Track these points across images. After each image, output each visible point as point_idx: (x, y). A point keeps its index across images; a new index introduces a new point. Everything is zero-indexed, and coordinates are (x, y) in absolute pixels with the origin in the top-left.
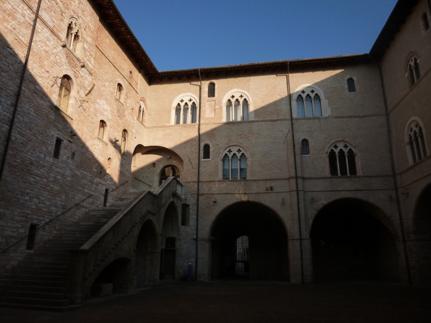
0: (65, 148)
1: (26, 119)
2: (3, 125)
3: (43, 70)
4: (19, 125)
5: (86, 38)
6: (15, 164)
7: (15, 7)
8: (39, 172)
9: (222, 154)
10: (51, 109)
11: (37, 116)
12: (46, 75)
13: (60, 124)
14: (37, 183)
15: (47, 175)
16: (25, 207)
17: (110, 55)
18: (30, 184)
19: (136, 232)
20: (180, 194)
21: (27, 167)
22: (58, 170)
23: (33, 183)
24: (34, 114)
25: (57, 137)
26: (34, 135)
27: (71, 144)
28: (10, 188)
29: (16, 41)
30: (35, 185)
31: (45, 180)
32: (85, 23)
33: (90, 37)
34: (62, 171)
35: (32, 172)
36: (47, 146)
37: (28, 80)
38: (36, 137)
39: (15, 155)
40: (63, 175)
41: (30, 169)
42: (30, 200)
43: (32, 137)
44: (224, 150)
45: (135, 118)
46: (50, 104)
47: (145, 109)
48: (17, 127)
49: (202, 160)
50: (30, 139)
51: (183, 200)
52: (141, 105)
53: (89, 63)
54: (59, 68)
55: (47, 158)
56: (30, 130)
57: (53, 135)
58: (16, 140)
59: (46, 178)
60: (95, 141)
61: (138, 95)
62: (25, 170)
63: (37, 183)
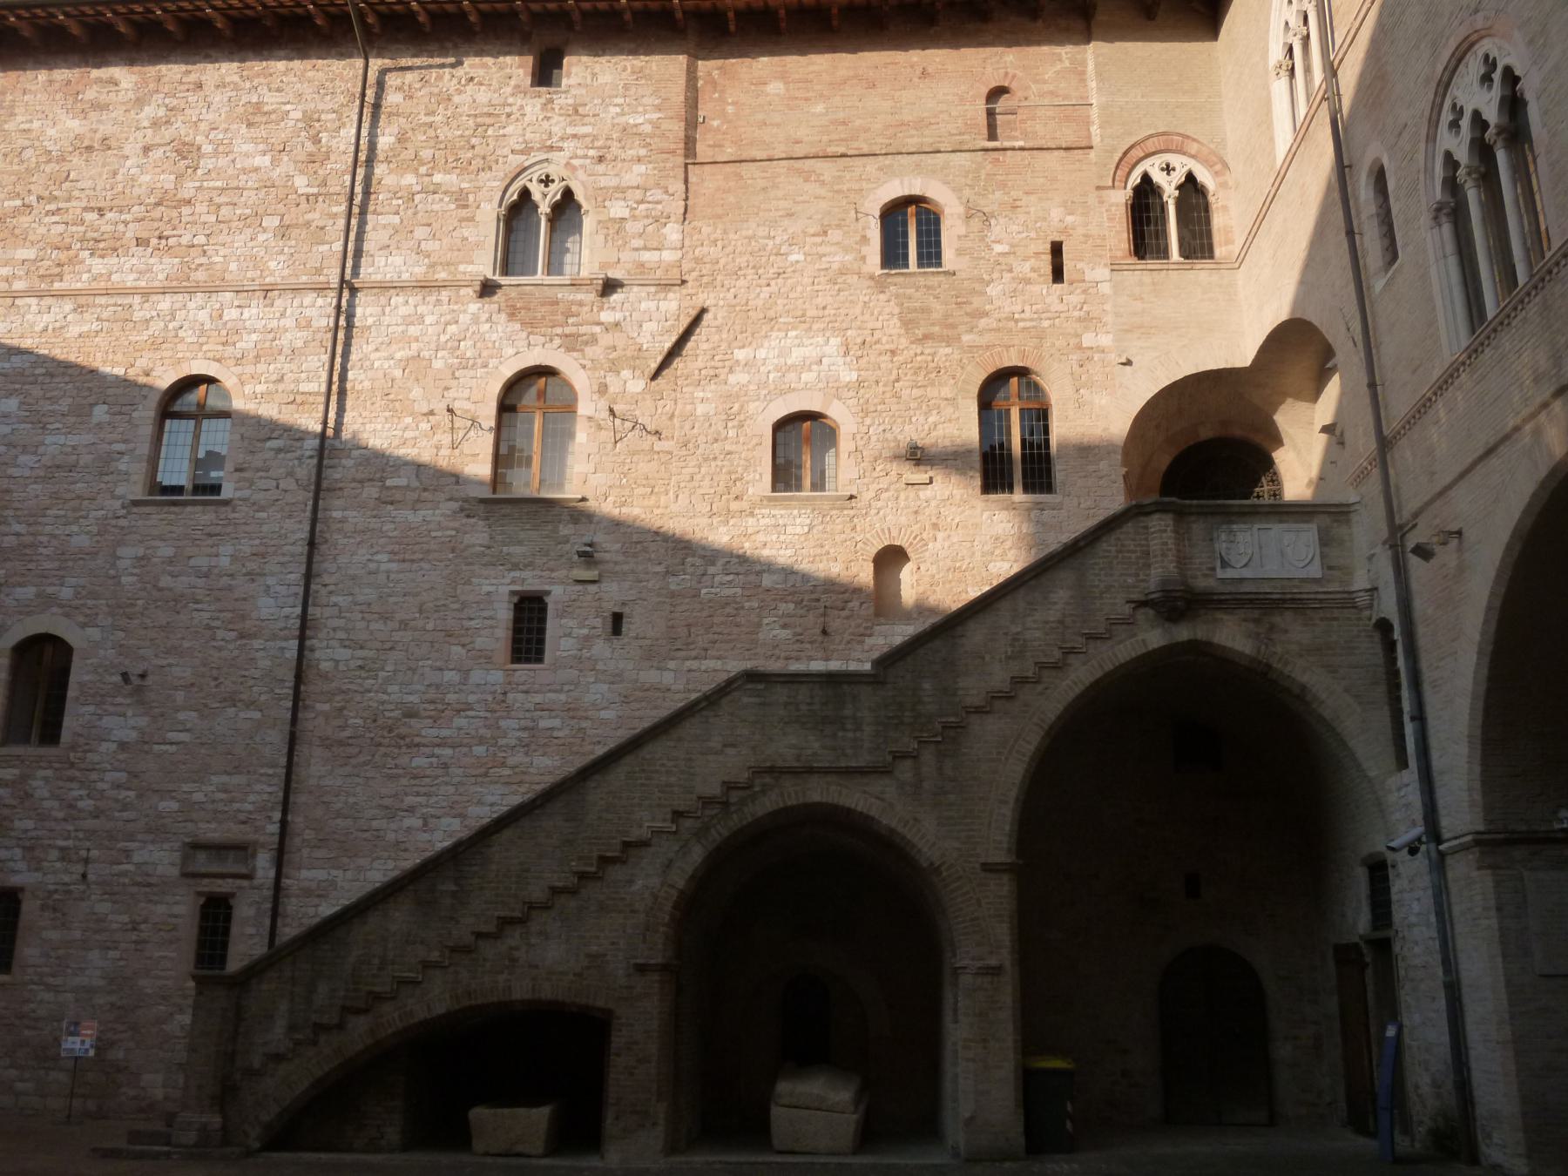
0: (561, 615)
2: (284, 644)
3: (409, 420)
4: (341, 623)
5: (614, 182)
6: (347, 733)
7: (274, 324)
8: (445, 733)
9: (1428, 171)
10: (468, 516)
11: (406, 566)
12: (424, 426)
13: (520, 543)
14: (445, 766)
15: (487, 733)
16: (406, 850)
17: (802, 133)
18: (415, 777)
19: (656, 880)
20: (1315, 571)
21: (390, 731)
22: (538, 698)
23: (428, 772)
24: (394, 566)
25: (513, 593)
26: (404, 625)
27: (592, 588)
28: (340, 805)
29: (293, 407)
30: (437, 777)
31: (479, 750)
32: (595, 138)
34: (563, 697)
35: (417, 740)
36: (466, 640)
37: (354, 480)
38: (415, 629)
39: (341, 709)
40: (571, 711)
41: (403, 730)
42: (425, 824)
43: (397, 636)
44: (1431, 138)
45: (1102, 273)
46: (455, 505)
47: (1204, 176)
48: (334, 630)
49: (1378, 285)
50: (388, 645)
51: (1362, 599)
52: (1158, 177)
53: (647, 256)
54: (480, 372)
55: (477, 676)
56: (385, 617)
57: (489, 593)
58: (336, 667)
59: (481, 741)
60: (751, 521)
61: (1092, 154)
62: (386, 741)
63: (445, 766)
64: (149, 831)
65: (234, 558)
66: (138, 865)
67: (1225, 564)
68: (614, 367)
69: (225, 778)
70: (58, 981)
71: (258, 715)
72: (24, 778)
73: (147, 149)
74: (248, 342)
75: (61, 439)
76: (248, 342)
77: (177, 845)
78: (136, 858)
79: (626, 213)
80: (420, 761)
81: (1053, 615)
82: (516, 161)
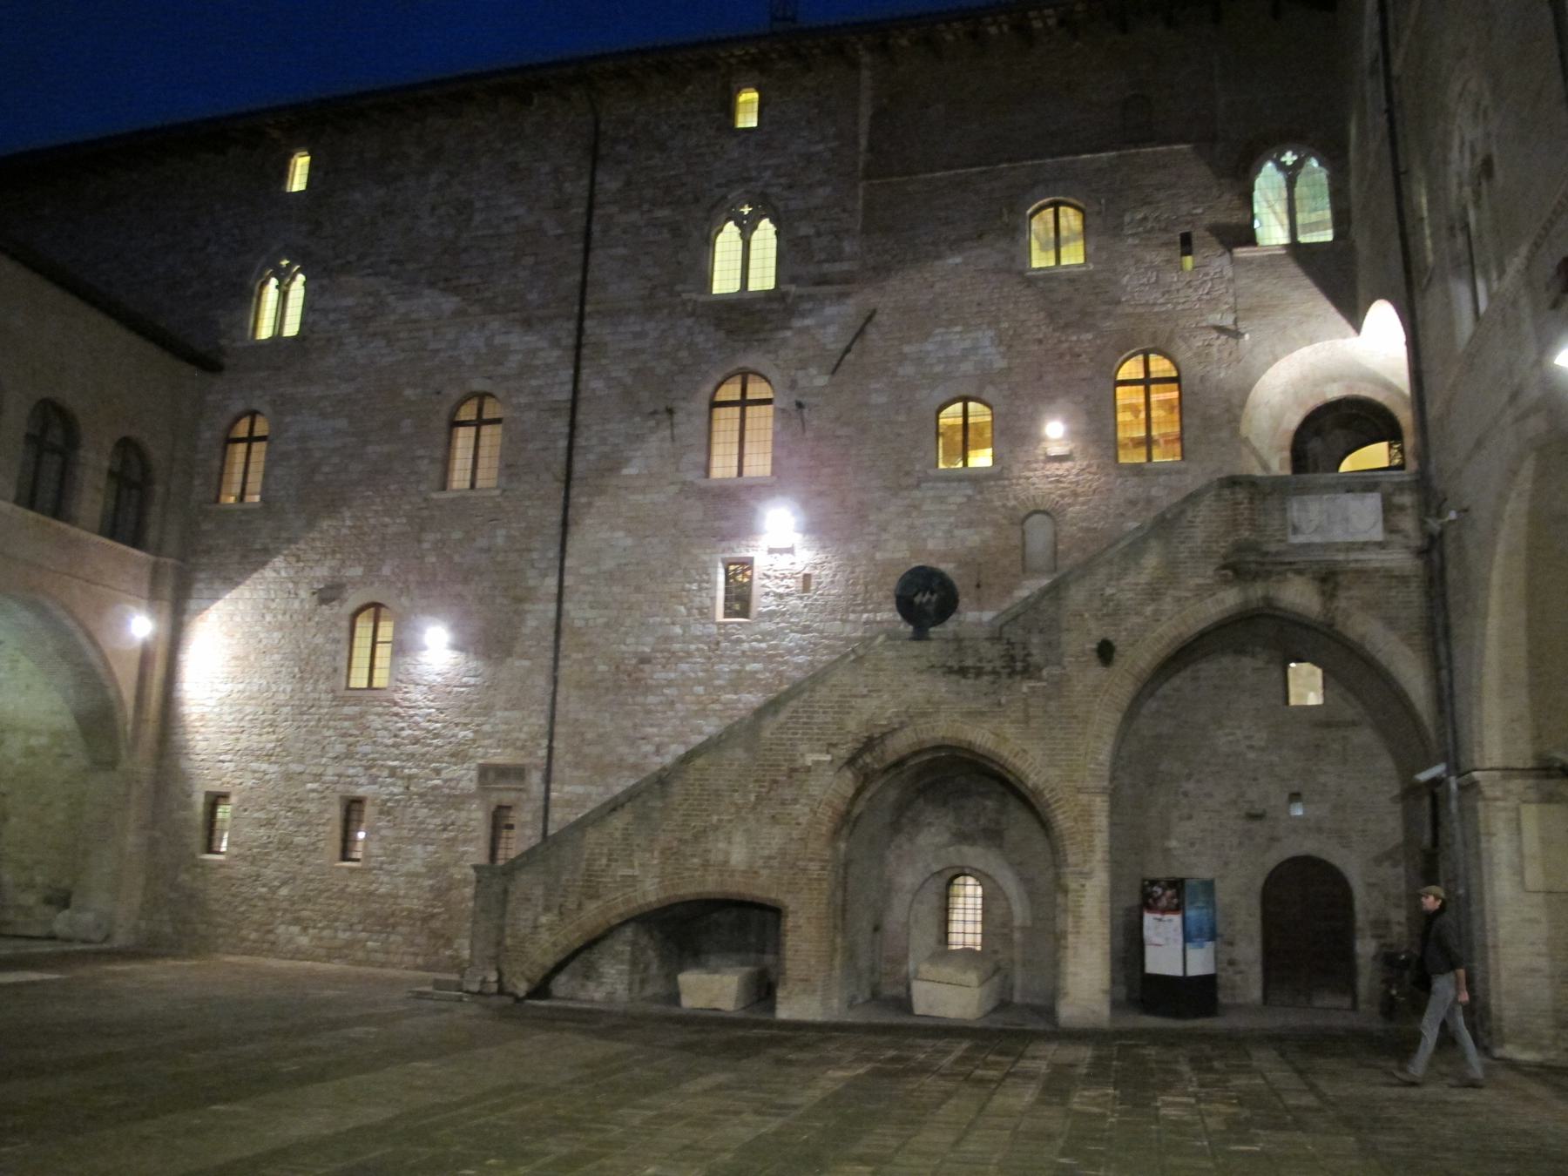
1: (609, 564)
8: (672, 675)
31: (700, 690)
33: (821, 183)
59: (699, 682)
63: (673, 703)
64: (452, 755)
65: (509, 537)
66: (446, 781)
67: (1296, 530)
68: (803, 365)
69: (507, 714)
70: (393, 867)
71: (527, 663)
72: (362, 715)
73: (433, 208)
74: (514, 361)
75: (378, 449)
76: (514, 361)
77: (474, 765)
78: (444, 775)
79: (812, 231)
80: (651, 699)
81: (1144, 578)
82: (718, 192)
